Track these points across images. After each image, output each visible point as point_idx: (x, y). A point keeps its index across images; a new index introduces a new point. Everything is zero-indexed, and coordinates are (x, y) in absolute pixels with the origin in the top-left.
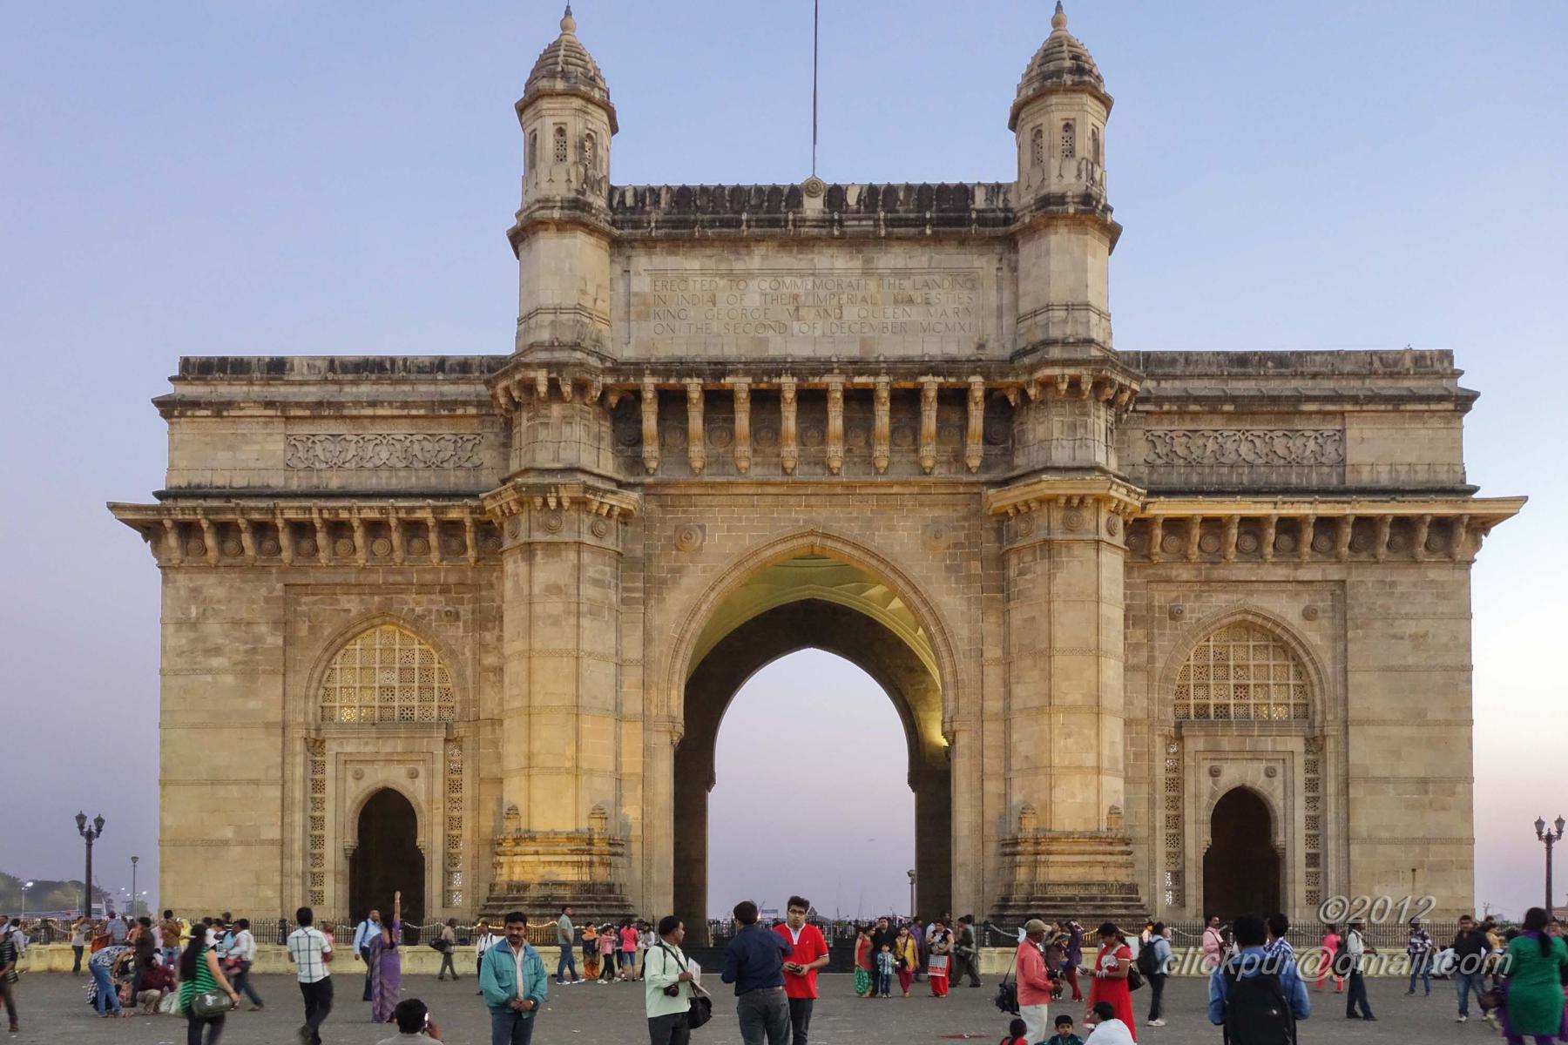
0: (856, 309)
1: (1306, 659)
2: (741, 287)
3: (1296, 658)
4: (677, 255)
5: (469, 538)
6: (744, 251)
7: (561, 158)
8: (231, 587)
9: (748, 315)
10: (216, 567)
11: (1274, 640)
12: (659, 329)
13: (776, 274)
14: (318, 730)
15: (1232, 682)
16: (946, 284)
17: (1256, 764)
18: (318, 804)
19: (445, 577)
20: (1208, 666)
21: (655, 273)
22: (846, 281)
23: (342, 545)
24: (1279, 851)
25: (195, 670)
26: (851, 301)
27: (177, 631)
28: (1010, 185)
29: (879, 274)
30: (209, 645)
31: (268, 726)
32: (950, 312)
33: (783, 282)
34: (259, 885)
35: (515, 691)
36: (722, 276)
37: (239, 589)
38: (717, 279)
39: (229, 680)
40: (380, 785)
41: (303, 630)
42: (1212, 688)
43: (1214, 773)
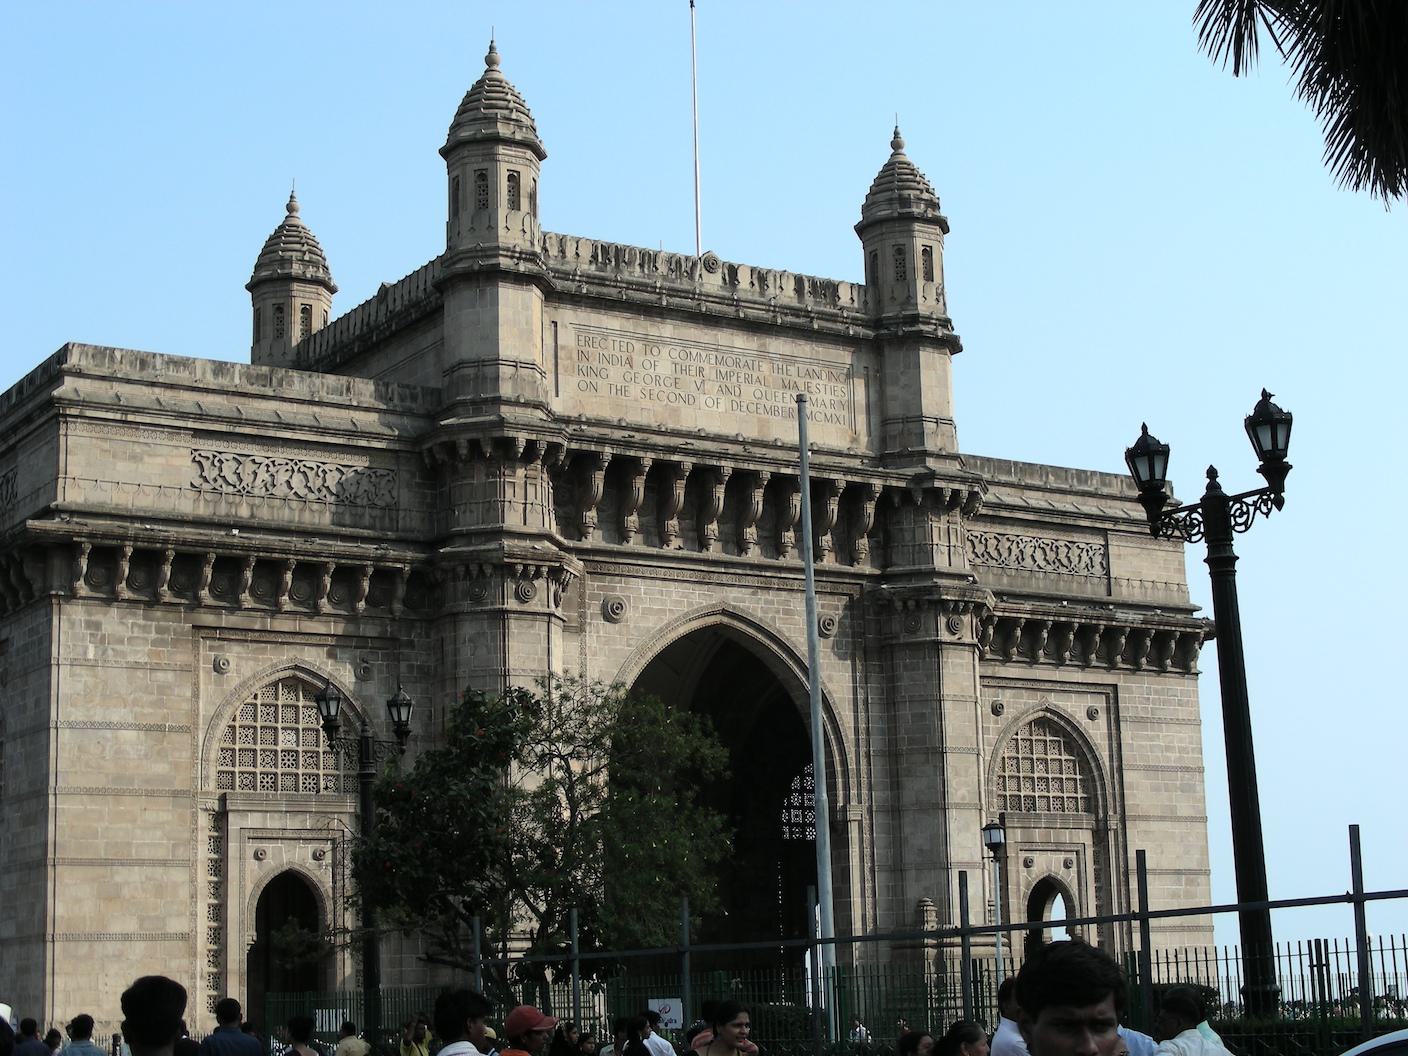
0: (752, 388)
5: (401, 590)
7: (515, 204)
11: (1064, 737)
13: (684, 343)
14: (223, 799)
18: (220, 889)
21: (581, 329)
26: (748, 380)
29: (771, 359)
32: (828, 404)
36: (638, 339)
37: (144, 629)
38: (633, 342)
40: (286, 868)
43: (1028, 864)
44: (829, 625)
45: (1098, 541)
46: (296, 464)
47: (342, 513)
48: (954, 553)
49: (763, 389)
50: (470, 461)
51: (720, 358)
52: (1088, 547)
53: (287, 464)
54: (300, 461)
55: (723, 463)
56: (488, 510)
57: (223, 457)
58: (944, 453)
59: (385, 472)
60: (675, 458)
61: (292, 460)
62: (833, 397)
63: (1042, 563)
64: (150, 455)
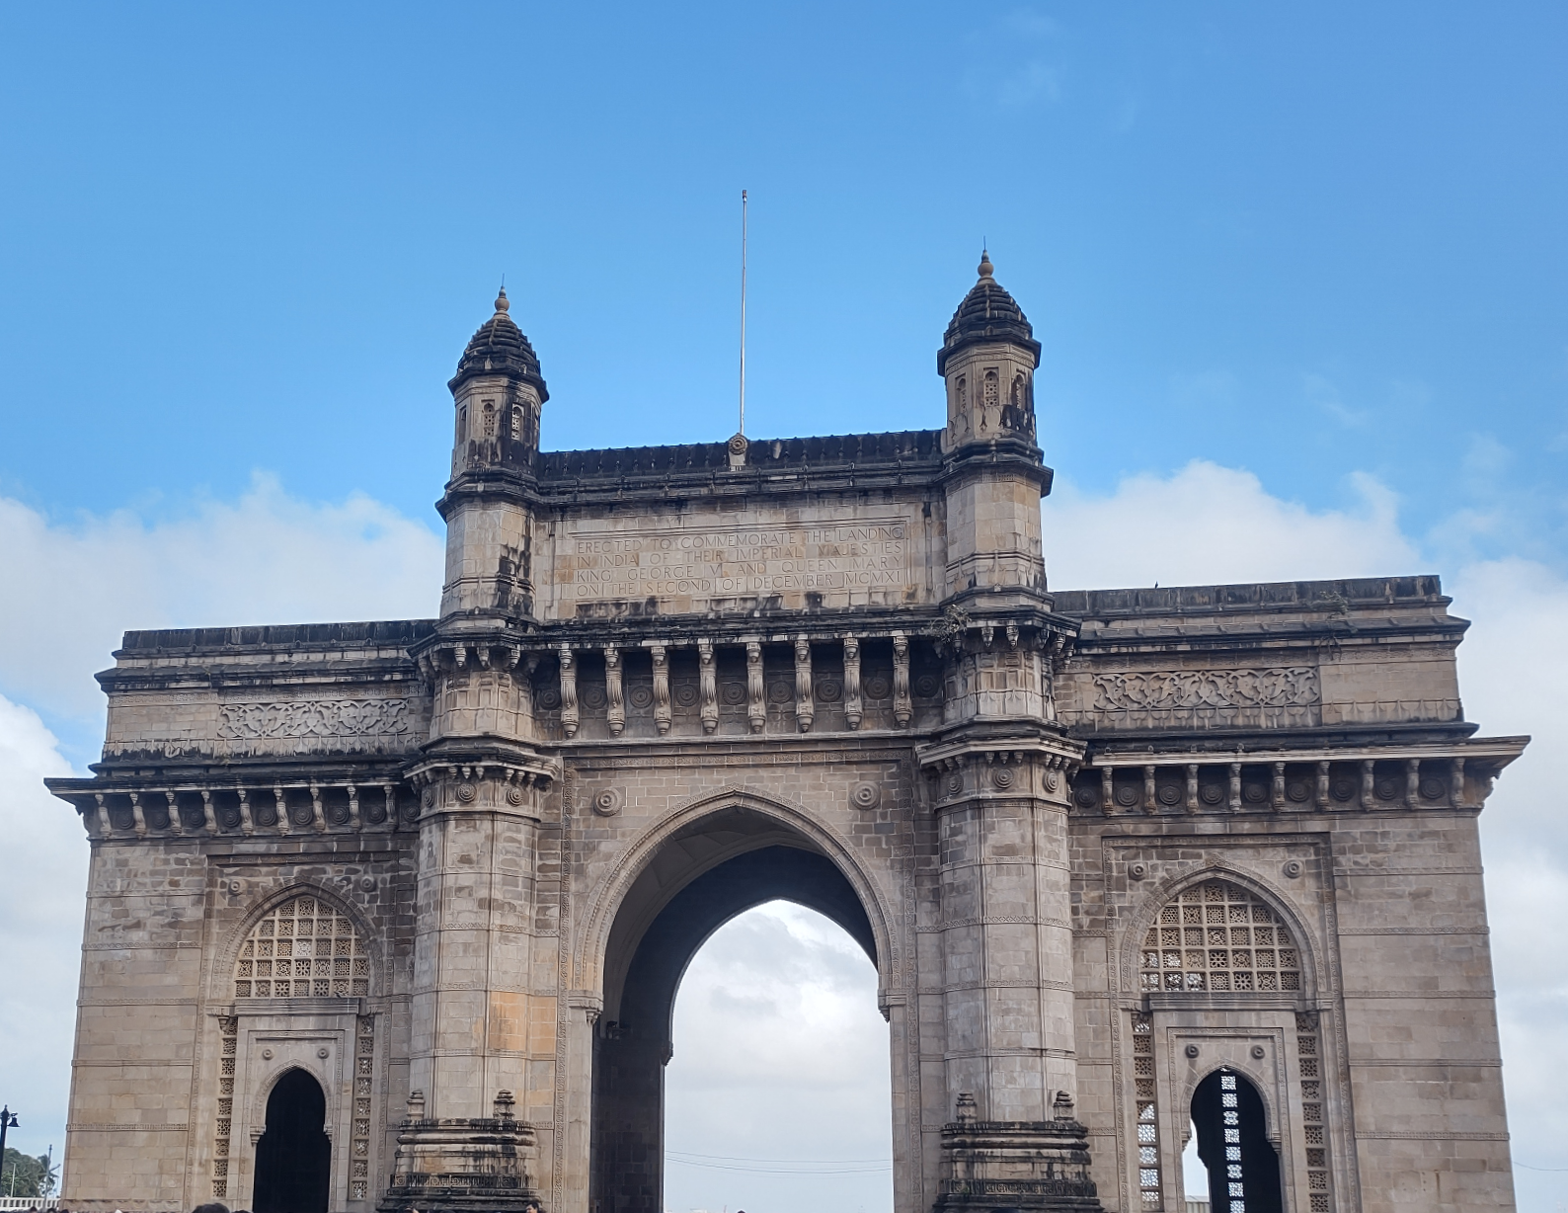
1: (1289, 921)
3: (1279, 919)
5: (389, 806)
8: (155, 859)
10: (144, 839)
15: (1207, 947)
17: (1239, 1042)
19: (365, 847)
20: (1178, 929)
23: (266, 814)
24: (1274, 1146)
25: (115, 945)
27: (100, 905)
28: (939, 432)
30: (131, 921)
31: (183, 1003)
34: (161, 1174)
35: (425, 967)
37: (166, 862)
39: (148, 954)
41: (221, 903)
42: (1184, 954)
43: (1191, 1054)
44: (865, 796)
45: (1298, 665)
46: (313, 705)
47: (354, 743)
48: (1011, 699)
50: (438, 678)
52: (1287, 672)
53: (305, 706)
54: (317, 702)
55: (700, 641)
57: (247, 708)
58: (998, 589)
59: (398, 702)
60: (645, 643)
61: (309, 702)
63: (1213, 700)
64: (181, 714)
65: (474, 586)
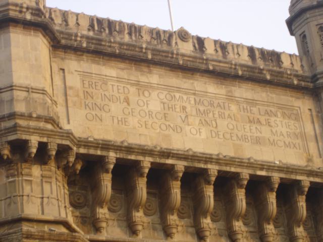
0: (226, 123)
2: (147, 96)
4: (99, 64)
6: (146, 69)
9: (154, 115)
12: (90, 116)
13: (169, 88)
16: (279, 115)
21: (84, 75)
22: (216, 102)
26: (222, 116)
29: (237, 101)
32: (285, 134)
33: (174, 96)
36: (132, 85)
38: (129, 86)
49: (234, 123)
51: (198, 100)
55: (209, 166)
56: (10, 204)
60: (170, 161)
62: (288, 130)
65: (24, 94)
